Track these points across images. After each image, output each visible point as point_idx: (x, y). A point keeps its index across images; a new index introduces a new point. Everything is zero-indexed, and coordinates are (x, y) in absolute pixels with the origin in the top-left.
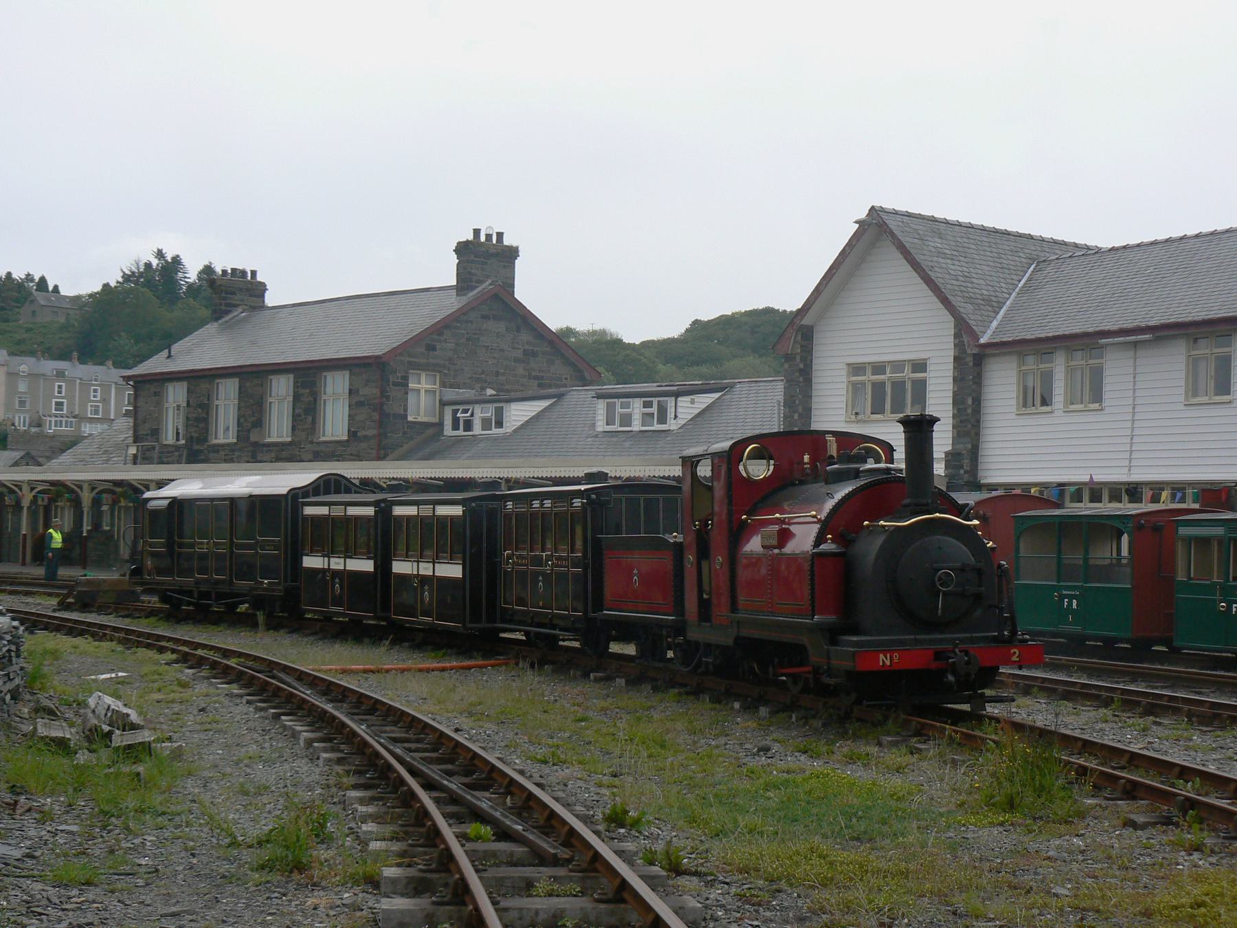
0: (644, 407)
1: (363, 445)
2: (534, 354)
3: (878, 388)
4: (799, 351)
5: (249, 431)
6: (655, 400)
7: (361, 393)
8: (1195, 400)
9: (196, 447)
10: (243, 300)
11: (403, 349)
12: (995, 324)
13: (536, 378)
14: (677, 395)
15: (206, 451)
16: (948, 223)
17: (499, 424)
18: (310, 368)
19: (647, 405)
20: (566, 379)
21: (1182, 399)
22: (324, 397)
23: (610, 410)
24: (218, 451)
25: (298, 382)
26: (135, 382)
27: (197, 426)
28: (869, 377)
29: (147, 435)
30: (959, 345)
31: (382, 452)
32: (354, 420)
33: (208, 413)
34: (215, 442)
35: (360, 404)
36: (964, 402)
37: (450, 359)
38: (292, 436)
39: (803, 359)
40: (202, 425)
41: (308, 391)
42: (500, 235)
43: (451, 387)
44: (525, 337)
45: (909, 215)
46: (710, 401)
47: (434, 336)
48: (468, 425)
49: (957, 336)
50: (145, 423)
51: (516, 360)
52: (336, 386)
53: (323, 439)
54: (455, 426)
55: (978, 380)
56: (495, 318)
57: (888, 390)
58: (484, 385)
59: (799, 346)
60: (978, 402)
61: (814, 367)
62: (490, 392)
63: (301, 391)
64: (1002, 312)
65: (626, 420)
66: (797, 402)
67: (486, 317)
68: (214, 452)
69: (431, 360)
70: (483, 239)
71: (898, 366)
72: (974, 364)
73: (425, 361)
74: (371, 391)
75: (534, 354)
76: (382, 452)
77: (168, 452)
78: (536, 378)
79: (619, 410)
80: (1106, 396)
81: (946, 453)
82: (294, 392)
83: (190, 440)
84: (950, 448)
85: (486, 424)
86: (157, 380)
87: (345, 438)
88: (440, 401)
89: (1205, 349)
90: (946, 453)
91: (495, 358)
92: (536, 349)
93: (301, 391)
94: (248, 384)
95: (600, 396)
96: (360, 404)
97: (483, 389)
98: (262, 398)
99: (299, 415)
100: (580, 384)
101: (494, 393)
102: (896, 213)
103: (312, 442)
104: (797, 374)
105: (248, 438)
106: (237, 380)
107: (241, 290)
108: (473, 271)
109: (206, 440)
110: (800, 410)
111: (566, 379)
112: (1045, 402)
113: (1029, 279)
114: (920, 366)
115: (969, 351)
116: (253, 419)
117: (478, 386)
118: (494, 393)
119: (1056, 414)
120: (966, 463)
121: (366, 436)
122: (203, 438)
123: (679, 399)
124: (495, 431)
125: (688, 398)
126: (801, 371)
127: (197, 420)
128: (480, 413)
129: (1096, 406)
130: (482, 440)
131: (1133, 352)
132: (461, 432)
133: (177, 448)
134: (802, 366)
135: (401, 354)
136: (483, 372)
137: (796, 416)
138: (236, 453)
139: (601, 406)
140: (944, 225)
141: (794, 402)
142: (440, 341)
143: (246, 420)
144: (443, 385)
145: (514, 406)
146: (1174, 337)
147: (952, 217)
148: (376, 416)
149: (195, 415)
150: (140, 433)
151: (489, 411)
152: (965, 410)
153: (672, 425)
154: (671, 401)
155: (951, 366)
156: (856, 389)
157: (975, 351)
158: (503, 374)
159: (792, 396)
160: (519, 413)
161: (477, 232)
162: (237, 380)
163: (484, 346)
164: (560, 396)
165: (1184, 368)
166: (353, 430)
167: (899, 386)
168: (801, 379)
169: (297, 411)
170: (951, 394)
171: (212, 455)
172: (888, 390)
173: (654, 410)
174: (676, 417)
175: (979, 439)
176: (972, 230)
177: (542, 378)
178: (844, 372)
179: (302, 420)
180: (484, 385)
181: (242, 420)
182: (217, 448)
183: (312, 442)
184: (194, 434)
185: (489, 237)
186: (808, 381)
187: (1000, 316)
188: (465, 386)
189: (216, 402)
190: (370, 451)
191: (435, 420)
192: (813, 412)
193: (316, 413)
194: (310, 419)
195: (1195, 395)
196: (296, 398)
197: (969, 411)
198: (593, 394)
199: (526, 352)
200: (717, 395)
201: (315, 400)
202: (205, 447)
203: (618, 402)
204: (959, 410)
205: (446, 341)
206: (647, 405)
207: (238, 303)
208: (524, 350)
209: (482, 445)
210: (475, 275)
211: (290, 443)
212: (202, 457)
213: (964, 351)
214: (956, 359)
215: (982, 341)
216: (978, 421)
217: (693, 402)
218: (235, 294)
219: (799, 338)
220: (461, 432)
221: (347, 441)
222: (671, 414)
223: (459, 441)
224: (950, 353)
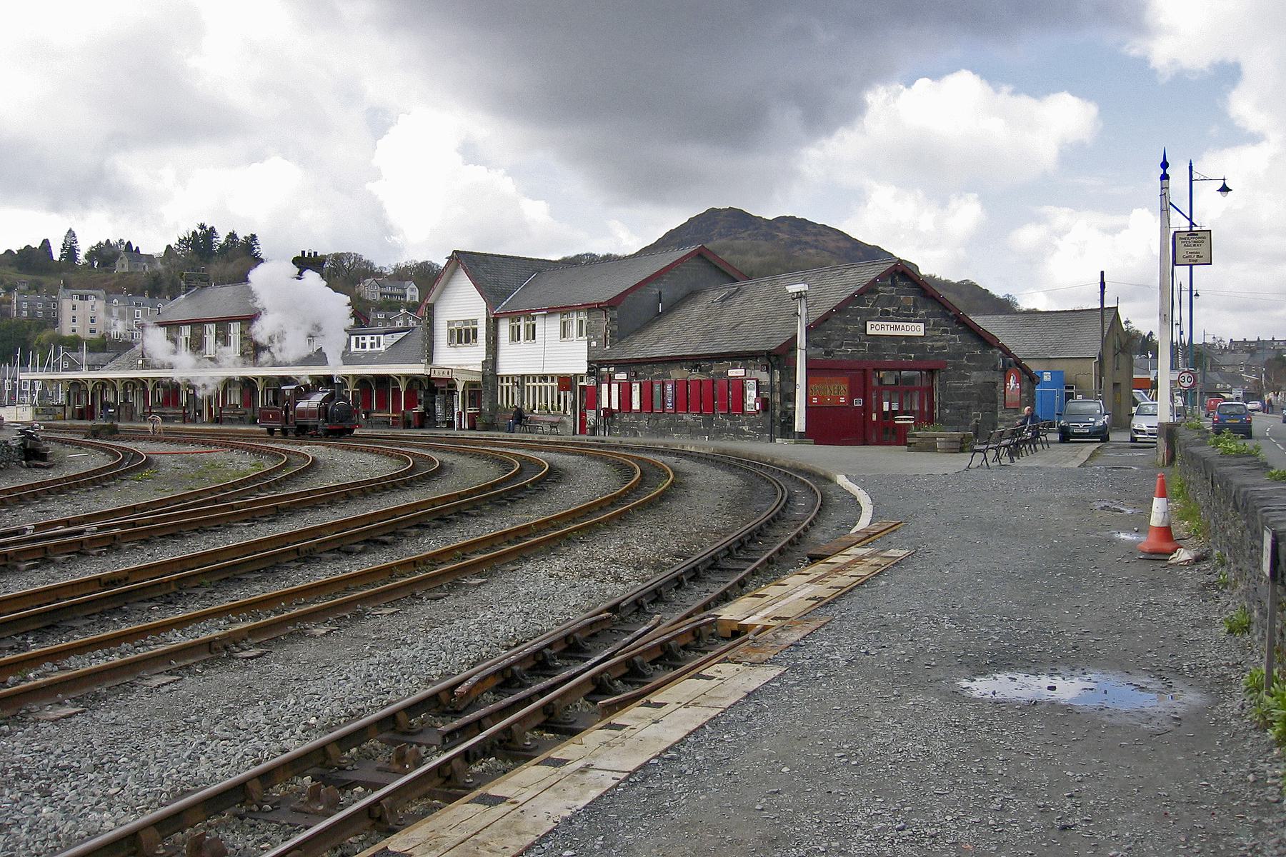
3: (460, 331)
6: (375, 336)
8: (565, 339)
12: (505, 303)
19: (372, 338)
22: (230, 335)
23: (357, 340)
28: (456, 326)
30: (487, 313)
35: (245, 338)
42: (315, 253)
57: (463, 332)
64: (510, 297)
65: (364, 346)
70: (306, 255)
71: (466, 322)
79: (361, 341)
80: (536, 337)
81: (483, 362)
84: (484, 359)
90: (483, 362)
96: (245, 338)
112: (519, 339)
114: (475, 322)
119: (522, 344)
120: (490, 366)
121: (248, 354)
125: (391, 335)
129: (534, 341)
146: (558, 312)
153: (383, 348)
156: (451, 332)
157: (493, 316)
161: (303, 252)
167: (467, 331)
172: (463, 332)
173: (375, 341)
185: (310, 254)
187: (508, 300)
195: (564, 337)
200: (406, 333)
203: (360, 337)
206: (372, 338)
215: (495, 312)
217: (393, 337)
222: (382, 344)
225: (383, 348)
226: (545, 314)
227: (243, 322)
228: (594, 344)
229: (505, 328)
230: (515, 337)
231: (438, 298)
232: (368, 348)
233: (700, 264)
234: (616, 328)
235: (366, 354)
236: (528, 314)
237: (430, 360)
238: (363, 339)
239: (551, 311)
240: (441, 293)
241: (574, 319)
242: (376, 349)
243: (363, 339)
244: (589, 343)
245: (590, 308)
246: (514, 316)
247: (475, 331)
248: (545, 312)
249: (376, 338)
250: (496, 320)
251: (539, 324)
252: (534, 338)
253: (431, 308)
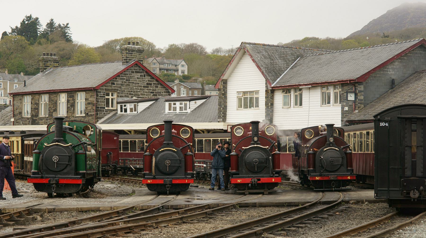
0: (180, 105)
1: (90, 118)
2: (150, 84)
3: (246, 99)
4: (222, 88)
5: (52, 113)
6: (183, 102)
7: (89, 100)
9: (34, 118)
10: (51, 64)
11: (102, 85)
13: (151, 93)
14: (190, 100)
15: (38, 120)
16: (269, 46)
17: (135, 110)
18: (73, 91)
19: (181, 104)
20: (162, 93)
21: (320, 105)
22: (77, 101)
23: (170, 105)
24: (42, 120)
25: (68, 96)
26: (13, 95)
27: (35, 111)
29: (18, 114)
31: (96, 120)
32: (87, 109)
33: (38, 107)
34: (40, 116)
35: (89, 104)
36: (268, 104)
37: (120, 87)
38: (67, 114)
39: (224, 90)
40: (36, 111)
41: (72, 99)
43: (121, 97)
44: (147, 78)
45: (255, 44)
46: (202, 102)
47: (115, 80)
48: (126, 111)
49: (266, 84)
50: (17, 110)
51: (144, 87)
52: (81, 99)
53: (77, 115)
54: (121, 111)
55: (272, 98)
56: (136, 72)
58: (132, 96)
59: (222, 86)
60: (272, 104)
61: (228, 93)
62: (134, 98)
63: (70, 99)
65: (175, 109)
66: (222, 104)
67: (133, 72)
68: (41, 120)
69: (113, 88)
72: (271, 93)
73: (111, 88)
74: (93, 99)
75: (150, 84)
76: (96, 120)
77: (25, 120)
78: (151, 93)
79: (173, 106)
82: (67, 99)
83: (32, 116)
85: (131, 110)
86: (21, 95)
87: (84, 115)
88: (117, 102)
89: (325, 90)
91: (136, 86)
92: (151, 83)
93: (70, 99)
94: (52, 96)
95: (167, 101)
96: (89, 104)
97: (132, 97)
98: (56, 101)
99: (69, 107)
100: (168, 94)
101: (137, 98)
102: (250, 44)
103: (73, 117)
104: (222, 95)
105: (52, 115)
106: (48, 95)
107: (50, 60)
108: (128, 56)
109: (38, 116)
110: (223, 106)
111: (162, 93)
113: (295, 64)
114: (257, 92)
115: (269, 89)
116: (54, 108)
117: (130, 96)
118: (137, 98)
119: (292, 108)
121: (91, 115)
122: (37, 115)
123: (191, 102)
124: (134, 112)
125: (194, 102)
126: (223, 94)
127: (35, 109)
128: (129, 106)
130: (130, 115)
131: (309, 90)
132: (123, 113)
133: (28, 118)
134: (223, 92)
135: (102, 86)
136: (132, 92)
137: (222, 109)
138: (48, 121)
139: (167, 104)
140: (268, 46)
141: (221, 104)
142: (116, 81)
143: (51, 109)
144: (118, 96)
145: (140, 104)
146: (318, 86)
147: (271, 44)
148: (94, 108)
149: (34, 107)
150: (16, 113)
151: (132, 106)
152: (269, 107)
154: (188, 102)
155: (265, 93)
156: (240, 100)
157: (271, 89)
158: (139, 92)
159: (220, 102)
160: (142, 106)
162: (48, 95)
163: (132, 82)
164: (156, 100)
165: (320, 96)
166: (87, 112)
168: (223, 97)
169: (68, 106)
170: (265, 102)
171: (40, 121)
173: (183, 105)
174: (190, 108)
175: (273, 116)
176: (278, 47)
177: (153, 93)
178: (236, 94)
179: (70, 109)
180: (132, 96)
181: (50, 109)
182: (42, 119)
183: (73, 117)
184: (33, 114)
186: (226, 97)
188: (125, 96)
189: (41, 103)
190: (93, 120)
191: (115, 109)
192: (228, 107)
193: (74, 107)
194: (72, 109)
196: (68, 101)
197: (270, 107)
198: (165, 100)
199: (147, 84)
200: (204, 100)
201: (74, 102)
202: (38, 118)
203: (172, 103)
204: (267, 107)
205: (118, 81)
206: (181, 104)
207: (49, 65)
208: (147, 83)
209: (129, 117)
210: (128, 57)
211: (66, 117)
212: (37, 122)
213: (268, 89)
214: (266, 91)
215: (272, 86)
216: (273, 110)
217: (196, 103)
218: (48, 62)
219: (222, 83)
220: (123, 113)
221: (85, 116)
222: (188, 107)
223: (122, 115)
224: (264, 89)
225: (189, 111)
226: (309, 88)
227: (88, 92)
228: (346, 109)
229: (279, 97)
230: (286, 104)
231: (230, 76)
232: (178, 111)
233: (421, 52)
234: (362, 97)
235: (176, 115)
236: (297, 88)
237: (224, 120)
238: (175, 104)
239: (314, 86)
240: (232, 72)
241: (331, 91)
242: (184, 111)
243: (175, 104)
244: (343, 108)
245: (343, 84)
246: (286, 89)
247: (257, 99)
248: (310, 86)
249: (183, 104)
250: (273, 91)
251: (306, 95)
252: (301, 104)
253: (225, 82)
